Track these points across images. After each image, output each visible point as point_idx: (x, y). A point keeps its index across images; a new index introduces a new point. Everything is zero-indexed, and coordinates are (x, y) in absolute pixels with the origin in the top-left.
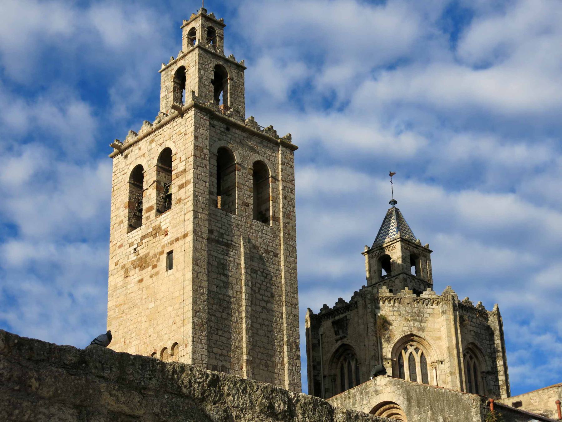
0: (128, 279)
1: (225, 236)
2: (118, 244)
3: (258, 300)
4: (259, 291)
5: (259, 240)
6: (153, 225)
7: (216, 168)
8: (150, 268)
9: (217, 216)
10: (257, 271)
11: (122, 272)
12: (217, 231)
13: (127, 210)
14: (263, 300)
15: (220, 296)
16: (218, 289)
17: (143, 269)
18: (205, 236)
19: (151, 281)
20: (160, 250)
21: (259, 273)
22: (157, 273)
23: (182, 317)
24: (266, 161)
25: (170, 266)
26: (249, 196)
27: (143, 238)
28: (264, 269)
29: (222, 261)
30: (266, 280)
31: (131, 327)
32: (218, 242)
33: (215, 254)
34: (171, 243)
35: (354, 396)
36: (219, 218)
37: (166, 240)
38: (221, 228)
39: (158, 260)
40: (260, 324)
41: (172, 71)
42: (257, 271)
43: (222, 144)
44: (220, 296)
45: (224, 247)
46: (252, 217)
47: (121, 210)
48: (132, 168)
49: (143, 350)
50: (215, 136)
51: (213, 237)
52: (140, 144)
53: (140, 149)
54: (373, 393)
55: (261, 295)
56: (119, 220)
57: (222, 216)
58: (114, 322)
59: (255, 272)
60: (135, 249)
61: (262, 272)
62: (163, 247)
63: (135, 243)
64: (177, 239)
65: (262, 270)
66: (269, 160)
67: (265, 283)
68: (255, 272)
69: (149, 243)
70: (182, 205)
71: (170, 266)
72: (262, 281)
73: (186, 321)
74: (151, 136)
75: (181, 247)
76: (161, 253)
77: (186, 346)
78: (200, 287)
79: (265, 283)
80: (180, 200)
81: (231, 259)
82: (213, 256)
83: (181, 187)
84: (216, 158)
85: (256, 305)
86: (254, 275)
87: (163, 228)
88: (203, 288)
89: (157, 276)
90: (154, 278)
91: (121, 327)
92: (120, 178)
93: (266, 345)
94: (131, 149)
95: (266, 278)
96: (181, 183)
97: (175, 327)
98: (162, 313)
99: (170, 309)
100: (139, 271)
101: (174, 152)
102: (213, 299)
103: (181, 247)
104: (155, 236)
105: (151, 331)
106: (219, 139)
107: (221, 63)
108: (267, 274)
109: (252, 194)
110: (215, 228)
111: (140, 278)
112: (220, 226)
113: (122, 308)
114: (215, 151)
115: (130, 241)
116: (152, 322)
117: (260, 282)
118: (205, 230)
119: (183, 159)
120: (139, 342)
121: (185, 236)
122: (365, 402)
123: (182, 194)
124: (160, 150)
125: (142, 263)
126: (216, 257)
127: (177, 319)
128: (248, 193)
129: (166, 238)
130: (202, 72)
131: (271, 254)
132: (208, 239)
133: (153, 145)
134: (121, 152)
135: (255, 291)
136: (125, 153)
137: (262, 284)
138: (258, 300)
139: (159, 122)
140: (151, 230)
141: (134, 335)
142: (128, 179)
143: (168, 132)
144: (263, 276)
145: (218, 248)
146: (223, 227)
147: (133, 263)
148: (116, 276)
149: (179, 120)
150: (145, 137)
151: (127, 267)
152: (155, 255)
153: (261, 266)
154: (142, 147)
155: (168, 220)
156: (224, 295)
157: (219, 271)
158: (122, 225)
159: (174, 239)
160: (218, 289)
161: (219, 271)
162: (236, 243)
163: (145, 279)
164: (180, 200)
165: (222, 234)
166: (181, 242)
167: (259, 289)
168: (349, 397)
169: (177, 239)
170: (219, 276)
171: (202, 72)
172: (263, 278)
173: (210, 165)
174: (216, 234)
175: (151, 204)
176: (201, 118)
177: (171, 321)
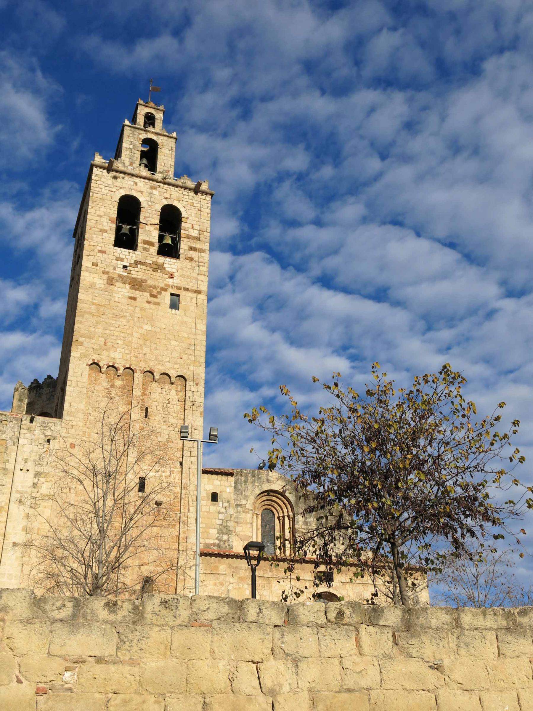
0: (111, 287)
2: (100, 249)
6: (154, 260)
8: (147, 294)
11: (105, 277)
13: (114, 226)
17: (137, 289)
19: (147, 306)
20: (162, 285)
22: (158, 304)
23: (192, 358)
25: (174, 305)
27: (137, 263)
31: (117, 334)
34: (179, 288)
35: (246, 476)
37: (170, 281)
39: (159, 293)
41: (140, 134)
47: (103, 220)
48: (123, 193)
49: (134, 362)
52: (137, 180)
53: (136, 184)
54: (265, 480)
56: (100, 226)
58: (87, 316)
60: (125, 267)
62: (168, 286)
63: (125, 260)
64: (187, 289)
69: (147, 272)
70: (193, 264)
71: (174, 305)
73: (197, 364)
74: (151, 182)
75: (191, 298)
76: (166, 290)
77: (197, 384)
80: (191, 259)
83: (192, 249)
87: (167, 269)
89: (157, 306)
90: (153, 306)
91: (100, 326)
92: (105, 191)
94: (123, 175)
96: (194, 246)
97: (179, 360)
98: (163, 342)
99: (174, 343)
100: (130, 288)
101: (184, 214)
103: (191, 298)
104: (155, 270)
105: (145, 350)
111: (131, 295)
113: (102, 309)
115: (118, 255)
116: (148, 343)
119: (197, 227)
120: (128, 352)
121: (198, 292)
122: (256, 484)
123: (193, 254)
124: (166, 202)
125: (137, 285)
127: (185, 357)
129: (171, 280)
133: (156, 192)
134: (109, 169)
136: (112, 174)
139: (165, 178)
140: (151, 262)
141: (120, 342)
142: (118, 200)
143: (177, 194)
147: (120, 276)
148: (96, 276)
149: (192, 194)
150: (145, 178)
151: (110, 275)
152: (155, 287)
154: (139, 184)
155: (176, 267)
158: (105, 234)
159: (183, 286)
163: (138, 299)
164: (191, 259)
166: (190, 294)
168: (241, 475)
169: (187, 289)
175: (152, 240)
177: (176, 355)
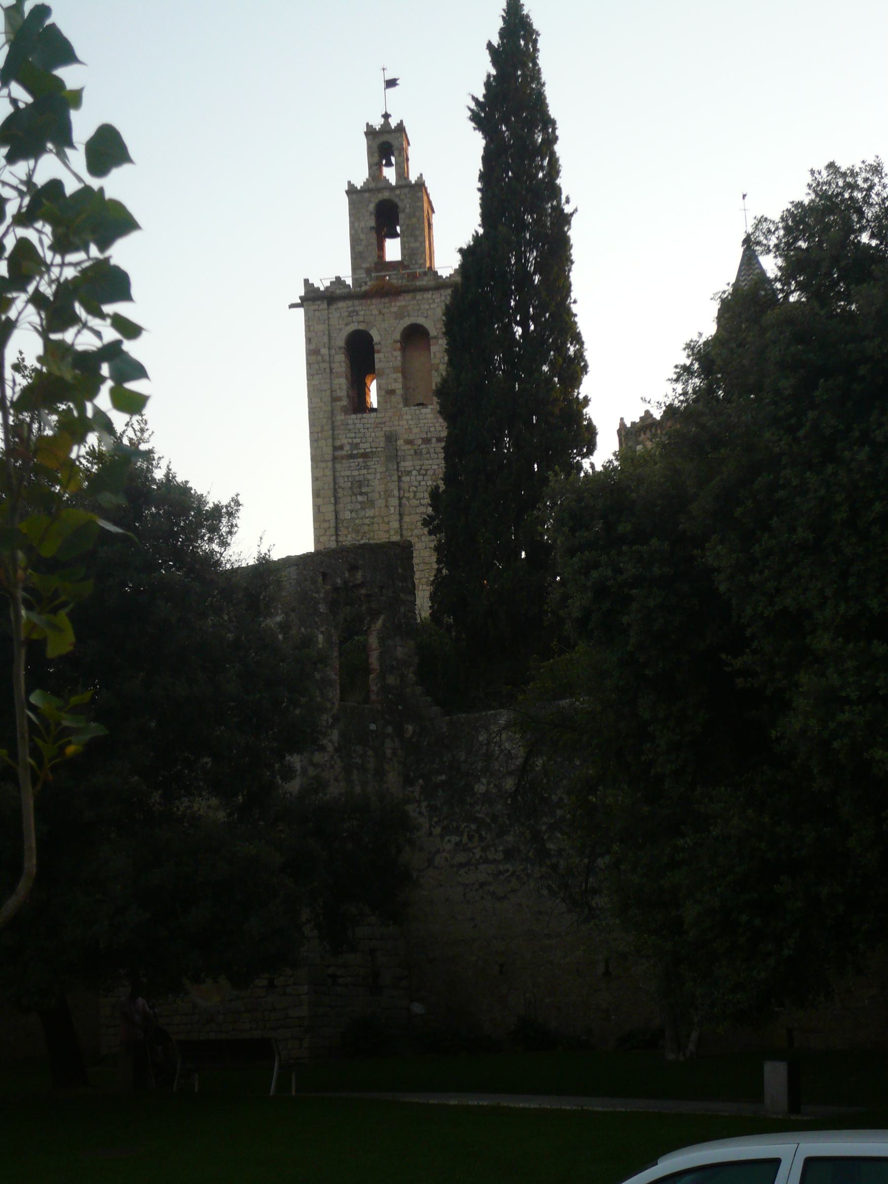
1: (361, 445)
3: (413, 507)
4: (415, 496)
5: (415, 430)
7: (343, 364)
9: (348, 424)
10: (411, 472)
12: (349, 443)
14: (421, 505)
15: (357, 521)
16: (353, 514)
18: (329, 457)
21: (414, 473)
24: (421, 321)
26: (395, 380)
28: (421, 465)
29: (357, 479)
30: (426, 478)
32: (351, 456)
33: (348, 473)
36: (351, 427)
38: (355, 437)
40: (418, 537)
42: (411, 472)
43: (353, 327)
44: (357, 521)
45: (361, 460)
46: (401, 405)
50: (341, 322)
51: (344, 453)
55: (417, 500)
57: (356, 421)
59: (409, 473)
61: (419, 471)
65: (418, 468)
66: (427, 317)
67: (423, 483)
68: (409, 473)
72: (420, 482)
78: (325, 521)
79: (423, 483)
81: (370, 471)
82: (343, 477)
84: (343, 350)
85: (410, 514)
86: (406, 479)
88: (329, 521)
93: (427, 560)
95: (424, 475)
102: (347, 528)
106: (347, 324)
107: (386, 195)
108: (427, 470)
109: (400, 375)
110: (345, 441)
112: (353, 435)
114: (340, 341)
117: (415, 483)
118: (329, 450)
126: (348, 477)
128: (394, 376)
130: (356, 224)
131: (434, 440)
132: (334, 459)
135: (408, 499)
137: (420, 485)
138: (413, 507)
144: (419, 474)
145: (352, 464)
146: (358, 435)
153: (419, 463)
156: (362, 518)
157: (353, 493)
160: (353, 514)
161: (353, 493)
162: (376, 448)
165: (357, 444)
167: (415, 492)
170: (354, 498)
171: (356, 224)
172: (420, 478)
173: (340, 362)
174: (347, 448)
176: (315, 311)
